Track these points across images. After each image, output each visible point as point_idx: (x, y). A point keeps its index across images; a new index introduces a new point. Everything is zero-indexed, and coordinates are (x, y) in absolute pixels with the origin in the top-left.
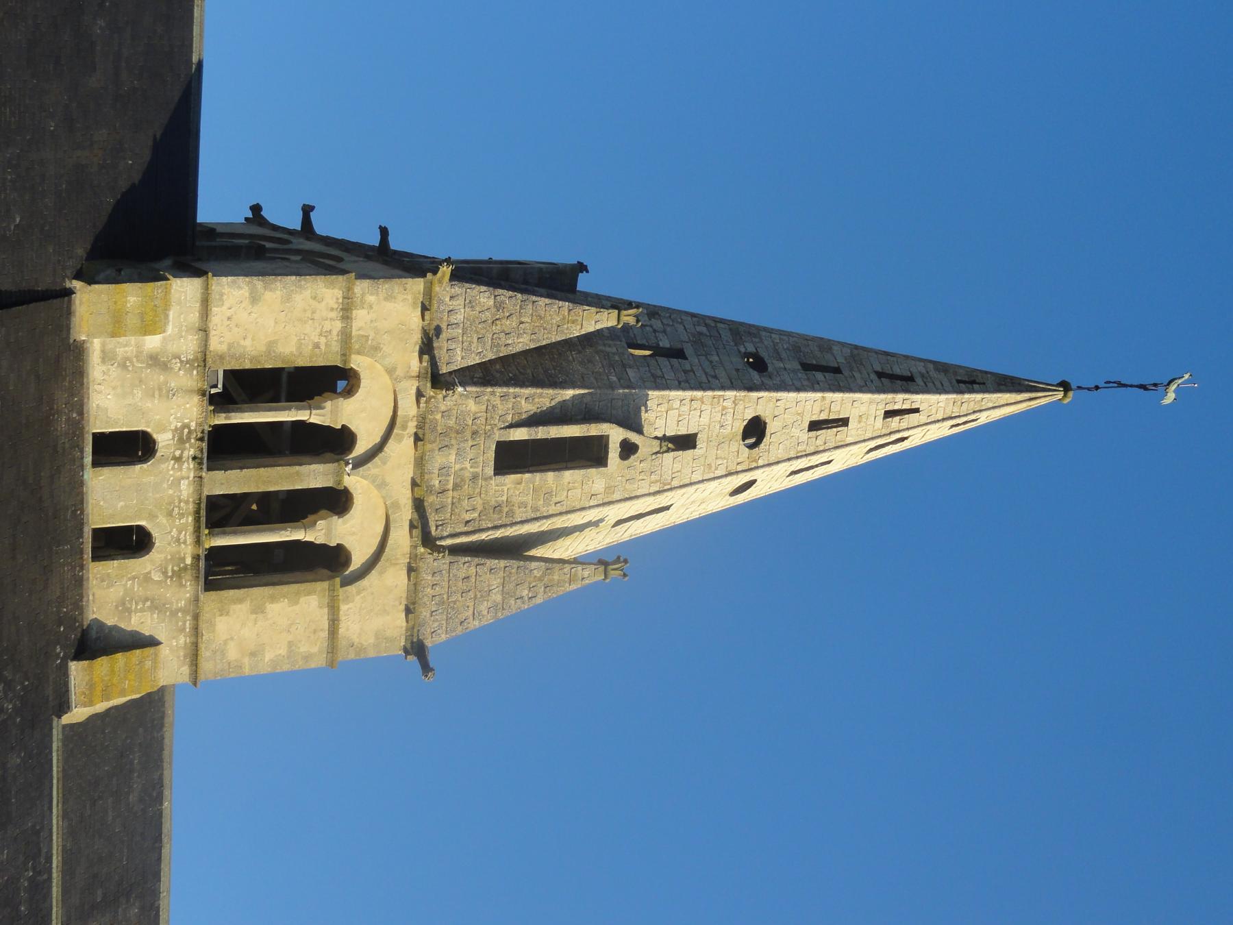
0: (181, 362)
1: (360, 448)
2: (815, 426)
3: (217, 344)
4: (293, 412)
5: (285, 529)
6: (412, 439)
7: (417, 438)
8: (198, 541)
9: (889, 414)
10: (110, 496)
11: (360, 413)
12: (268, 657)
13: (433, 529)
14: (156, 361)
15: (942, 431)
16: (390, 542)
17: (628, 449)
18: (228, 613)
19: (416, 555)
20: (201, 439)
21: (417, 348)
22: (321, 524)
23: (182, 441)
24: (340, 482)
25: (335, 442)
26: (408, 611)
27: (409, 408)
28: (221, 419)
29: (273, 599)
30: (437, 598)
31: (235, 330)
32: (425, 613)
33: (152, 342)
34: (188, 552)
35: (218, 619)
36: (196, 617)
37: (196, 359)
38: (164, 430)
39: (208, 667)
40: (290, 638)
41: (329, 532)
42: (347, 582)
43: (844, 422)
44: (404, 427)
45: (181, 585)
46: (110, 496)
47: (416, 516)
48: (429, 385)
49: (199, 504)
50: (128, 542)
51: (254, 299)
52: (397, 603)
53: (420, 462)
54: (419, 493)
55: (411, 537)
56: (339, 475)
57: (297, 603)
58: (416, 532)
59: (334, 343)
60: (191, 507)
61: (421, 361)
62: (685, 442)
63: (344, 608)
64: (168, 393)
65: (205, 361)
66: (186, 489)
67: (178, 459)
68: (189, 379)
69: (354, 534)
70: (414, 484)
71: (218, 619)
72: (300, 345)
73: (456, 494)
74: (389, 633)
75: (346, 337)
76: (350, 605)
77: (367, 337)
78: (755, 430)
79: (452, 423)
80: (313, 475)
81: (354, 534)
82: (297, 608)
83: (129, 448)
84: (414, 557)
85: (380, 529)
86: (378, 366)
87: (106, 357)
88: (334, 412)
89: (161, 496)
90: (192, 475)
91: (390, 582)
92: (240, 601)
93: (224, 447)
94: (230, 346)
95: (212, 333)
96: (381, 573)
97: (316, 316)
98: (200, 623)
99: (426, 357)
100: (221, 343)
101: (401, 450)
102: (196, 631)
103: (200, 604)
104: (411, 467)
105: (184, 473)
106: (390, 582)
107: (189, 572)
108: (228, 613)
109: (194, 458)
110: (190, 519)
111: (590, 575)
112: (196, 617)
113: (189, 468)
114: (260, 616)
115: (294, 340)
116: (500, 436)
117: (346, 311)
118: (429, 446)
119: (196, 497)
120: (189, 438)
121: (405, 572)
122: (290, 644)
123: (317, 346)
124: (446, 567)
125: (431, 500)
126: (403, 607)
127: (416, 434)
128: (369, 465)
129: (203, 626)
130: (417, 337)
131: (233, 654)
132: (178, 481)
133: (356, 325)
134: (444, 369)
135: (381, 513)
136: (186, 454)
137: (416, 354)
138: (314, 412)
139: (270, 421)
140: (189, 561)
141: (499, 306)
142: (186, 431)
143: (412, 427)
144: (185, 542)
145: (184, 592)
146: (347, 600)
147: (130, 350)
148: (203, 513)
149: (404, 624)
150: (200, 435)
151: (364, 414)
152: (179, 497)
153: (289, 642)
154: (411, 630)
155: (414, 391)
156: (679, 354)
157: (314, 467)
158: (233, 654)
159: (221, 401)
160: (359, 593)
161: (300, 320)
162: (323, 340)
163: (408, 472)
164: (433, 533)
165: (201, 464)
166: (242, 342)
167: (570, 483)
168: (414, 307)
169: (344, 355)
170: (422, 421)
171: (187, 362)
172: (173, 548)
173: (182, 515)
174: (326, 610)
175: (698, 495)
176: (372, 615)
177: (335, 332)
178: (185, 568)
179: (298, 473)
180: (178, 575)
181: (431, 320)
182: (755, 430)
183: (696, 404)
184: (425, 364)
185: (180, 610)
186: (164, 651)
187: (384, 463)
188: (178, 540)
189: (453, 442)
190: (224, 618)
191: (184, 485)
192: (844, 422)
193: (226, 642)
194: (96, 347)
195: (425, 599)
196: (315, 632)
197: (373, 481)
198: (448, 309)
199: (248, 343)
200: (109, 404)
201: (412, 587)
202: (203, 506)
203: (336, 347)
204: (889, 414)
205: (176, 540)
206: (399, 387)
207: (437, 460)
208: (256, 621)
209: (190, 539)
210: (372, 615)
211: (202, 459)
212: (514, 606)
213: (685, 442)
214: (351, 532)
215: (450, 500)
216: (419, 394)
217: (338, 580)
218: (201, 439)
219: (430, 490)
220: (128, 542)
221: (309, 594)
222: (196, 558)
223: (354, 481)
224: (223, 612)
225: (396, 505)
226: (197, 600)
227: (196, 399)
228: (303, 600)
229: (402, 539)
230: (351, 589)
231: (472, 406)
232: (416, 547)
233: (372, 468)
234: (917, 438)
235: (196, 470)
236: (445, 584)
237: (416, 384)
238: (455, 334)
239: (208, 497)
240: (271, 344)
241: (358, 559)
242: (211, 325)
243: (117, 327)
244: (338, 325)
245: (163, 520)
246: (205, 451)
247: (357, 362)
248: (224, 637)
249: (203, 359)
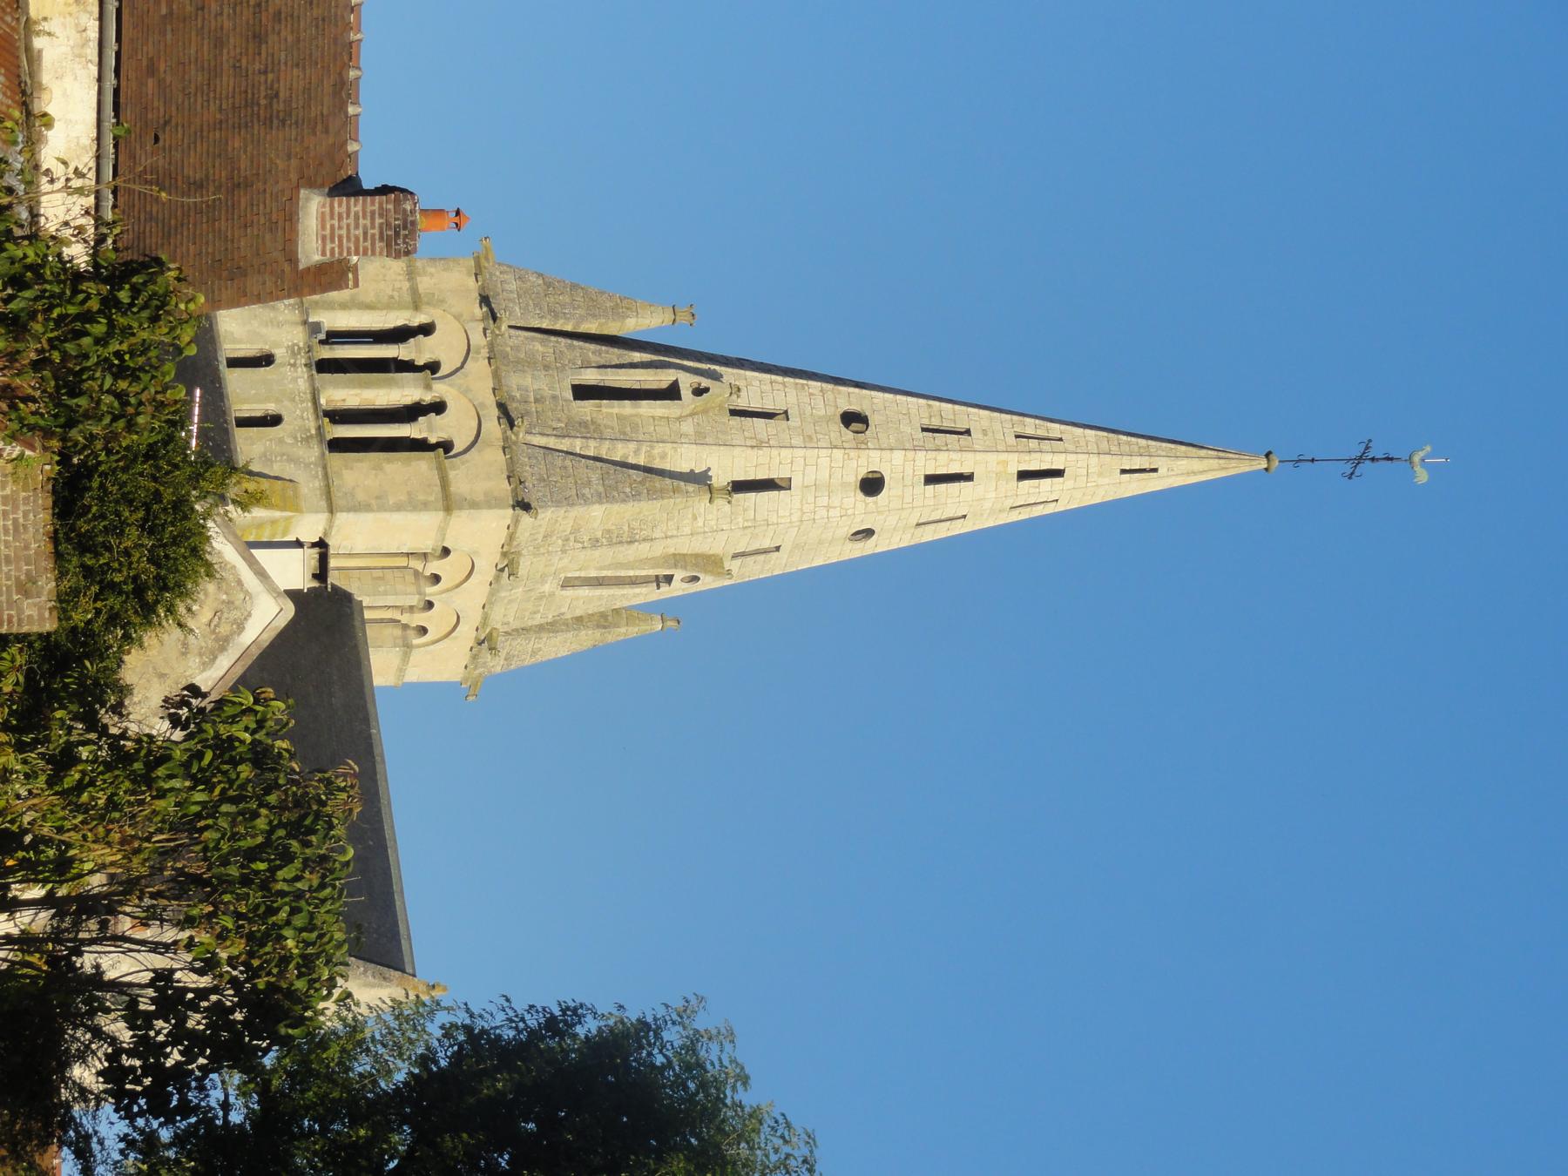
23: (294, 354)
27: (478, 339)
36: (325, 468)
38: (279, 345)
44: (478, 352)
67: (294, 365)
75: (414, 291)
85: (475, 424)
102: (326, 476)
112: (325, 468)
117: (411, 274)
122: (409, 493)
132: (295, 380)
143: (485, 353)
145: (314, 452)
168: (469, 274)
172: (299, 422)
180: (307, 439)
183: (776, 386)
191: (301, 382)
205: (299, 418)
214: (451, 426)
227: (301, 328)
237: (481, 326)
244: (407, 285)
245: (286, 403)
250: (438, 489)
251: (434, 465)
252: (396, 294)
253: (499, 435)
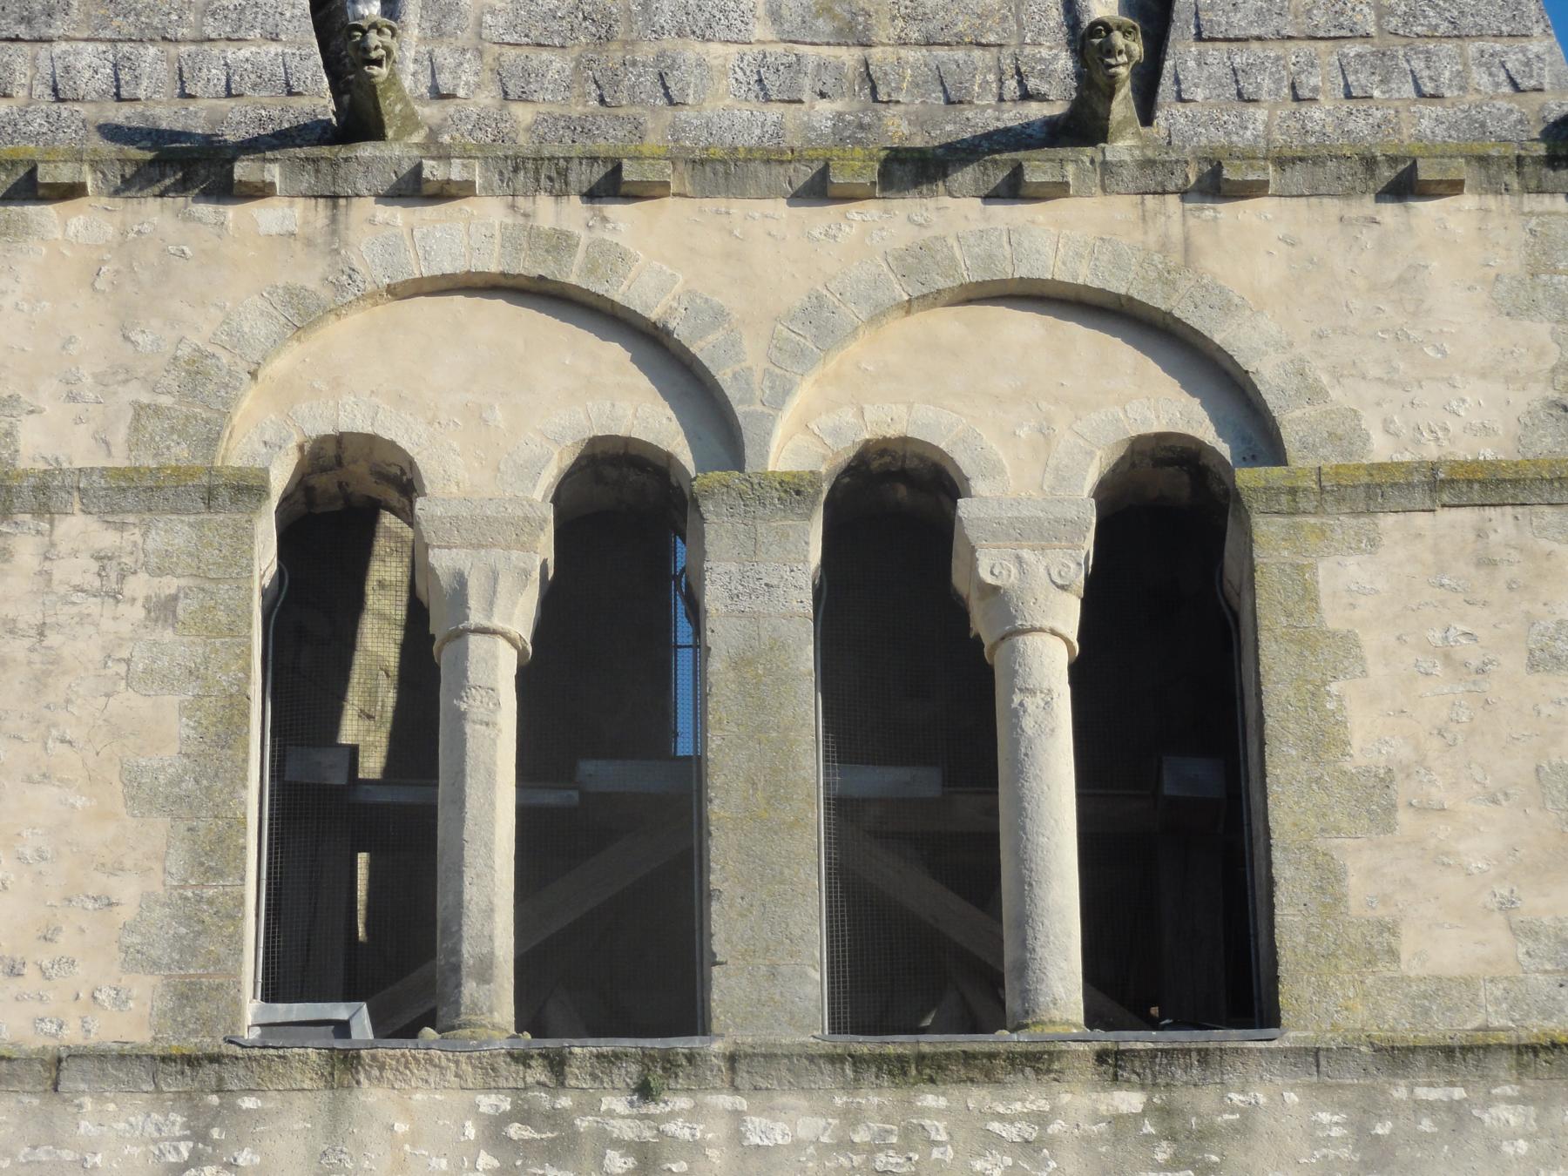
0: (196, 1160)
1: (649, 418)
3: (130, 1015)
4: (473, 704)
5: (1015, 715)
6: (615, 210)
7: (610, 187)
8: (1038, 1063)
13: (1036, 111)
16: (1084, 275)
18: (1390, 928)
19: (1147, 164)
20: (557, 1064)
21: (205, 210)
22: (991, 564)
24: (793, 490)
25: (624, 533)
26: (1405, 186)
27: (472, 234)
28: (493, 999)
29: (1325, 739)
30: (1359, 80)
31: (66, 943)
32: (1423, 126)
34: (1083, 1106)
35: (1409, 966)
36: (1396, 1056)
37: (189, 1099)
40: (1512, 662)
41: (1042, 533)
42: (1261, 434)
44: (560, 242)
45: (1245, 1127)
47: (966, 176)
48: (366, 150)
49: (858, 1061)
52: (1368, 236)
53: (719, 170)
54: (855, 168)
55: (1059, 190)
57: (1347, 643)
58: (1038, 169)
59: (156, 540)
60: (876, 1098)
61: (260, 191)
63: (1381, 449)
65: (191, 1061)
66: (792, 1123)
69: (1045, 432)
70: (819, 190)
71: (1409, 966)
72: (153, 679)
73: (884, 31)
74: (1510, 261)
75: (128, 493)
76: (1371, 423)
77: (140, 410)
79: (557, 64)
80: (760, 594)
81: (1045, 432)
82: (1371, 642)
84: (1153, 178)
85: (1025, 328)
86: (279, 366)
88: (482, 530)
90: (725, 1101)
91: (1262, 272)
92: (1329, 877)
94: (137, 960)
95: (73, 1036)
96: (1227, 307)
97: (28, 616)
98: (1424, 1036)
99: (243, 170)
100: (120, 999)
101: (654, 254)
103: (1333, 1040)
104: (738, 207)
105: (712, 1132)
106: (1262, 272)
107: (1182, 1097)
108: (1390, 928)
109: (645, 1091)
110: (931, 1100)
112: (1396, 1056)
113: (695, 1117)
114: (1402, 791)
115: (130, 702)
118: (655, 140)
119: (826, 1078)
120: (554, 1118)
121: (1226, 210)
123: (163, 610)
124: (1215, 53)
125: (899, 128)
126: (1390, 212)
127: (592, 195)
128: (724, 376)
129: (1443, 1027)
130: (159, 217)
133: (80, 452)
134: (320, 102)
135: (950, 323)
136: (626, 1130)
137: (232, 213)
138: (476, 618)
140: (1130, 1101)
142: (515, 1131)
143: (570, 215)
144: (1041, 1119)
146: (1347, 435)
148: (898, 1044)
149: (1468, 201)
150: (538, 1073)
151: (499, 416)
152: (824, 1150)
153: (1533, 666)
154: (1496, 168)
155: (399, 216)
157: (714, 598)
160: (1315, 393)
161: (40, 682)
162: (139, 586)
163: (770, 223)
164: (1058, 108)
165: (669, 1063)
166: (127, 913)
169: (210, 497)
170: (532, 170)
171: (199, 1136)
173: (914, 1136)
174: (1388, 521)
177: (108, 539)
178: (1165, 1113)
179: (740, 663)
181: (77, 157)
184: (273, 173)
185: (1361, 1133)
187: (719, 316)
188: (1028, 1147)
189: (646, 52)
190: (1408, 944)
191: (765, 1130)
193: (1525, 931)
195: (1360, 125)
196: (1486, 562)
197: (799, 355)
198: (46, 103)
199: (128, 891)
201: (1297, 175)
202: (865, 1045)
206: (373, 268)
207: (723, 105)
208: (1423, 809)
209: (1028, 1098)
211: (646, 1059)
215: (912, 55)
216: (412, 189)
217: (1247, 478)
218: (557, 1064)
219: (848, 132)
221: (1309, 595)
222: (1112, 1065)
223: (804, 432)
224: (1378, 946)
225: (911, 261)
226: (1313, 1056)
227: (371, 1095)
228: (1334, 618)
229: (1079, 230)
230: (1293, 422)
232: (1106, 168)
233: (737, 367)
235: (700, 1085)
236: (1295, 53)
238: (164, 71)
239: (836, 1028)
240: (142, 793)
241: (1171, 408)
242: (34, 1042)
246: (607, 1045)
247: (267, 442)
248: (1499, 938)
249: (190, 1069)
250: (1502, 522)
251: (1344, 524)
252: (139, 586)
253: (1122, 207)
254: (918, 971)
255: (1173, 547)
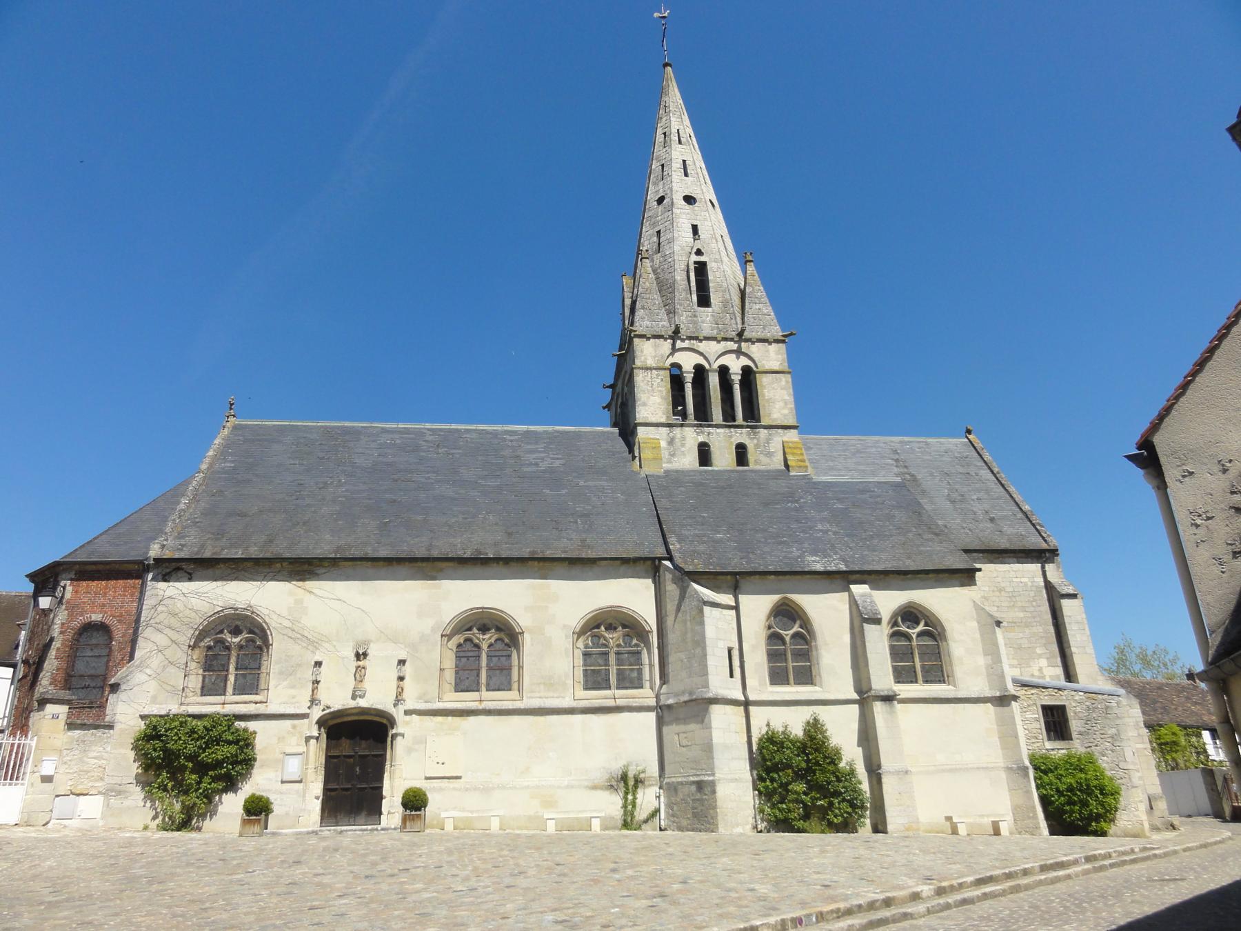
1: (702, 361)
2: (686, 175)
9: (680, 142)
10: (723, 459)
11: (688, 362)
12: (787, 397)
14: (671, 442)
15: (686, 117)
17: (699, 252)
25: (700, 372)
33: (663, 444)
39: (792, 421)
43: (684, 161)
46: (723, 459)
50: (741, 454)
51: (645, 404)
53: (707, 339)
56: (714, 371)
62: (695, 229)
64: (684, 439)
68: (677, 430)
78: (689, 200)
80: (714, 380)
83: (704, 454)
87: (670, 462)
89: (722, 441)
91: (755, 350)
93: (703, 414)
111: (751, 268)
116: (696, 306)
125: (722, 335)
131: (786, 411)
139: (692, 396)
141: (643, 308)
147: (667, 453)
156: (659, 232)
158: (786, 411)
159: (684, 415)
167: (714, 278)
175: (714, 223)
176: (770, 357)
182: (689, 200)
186: (785, 439)
192: (684, 161)
194: (666, 466)
200: (689, 460)
203: (662, 372)
204: (680, 142)
205: (741, 436)
210: (770, 357)
212: (765, 299)
213: (695, 229)
214: (736, 366)
220: (741, 454)
231: (683, 318)
234: (690, 130)
243: (657, 459)
254: (729, 415)
255: (748, 373)
